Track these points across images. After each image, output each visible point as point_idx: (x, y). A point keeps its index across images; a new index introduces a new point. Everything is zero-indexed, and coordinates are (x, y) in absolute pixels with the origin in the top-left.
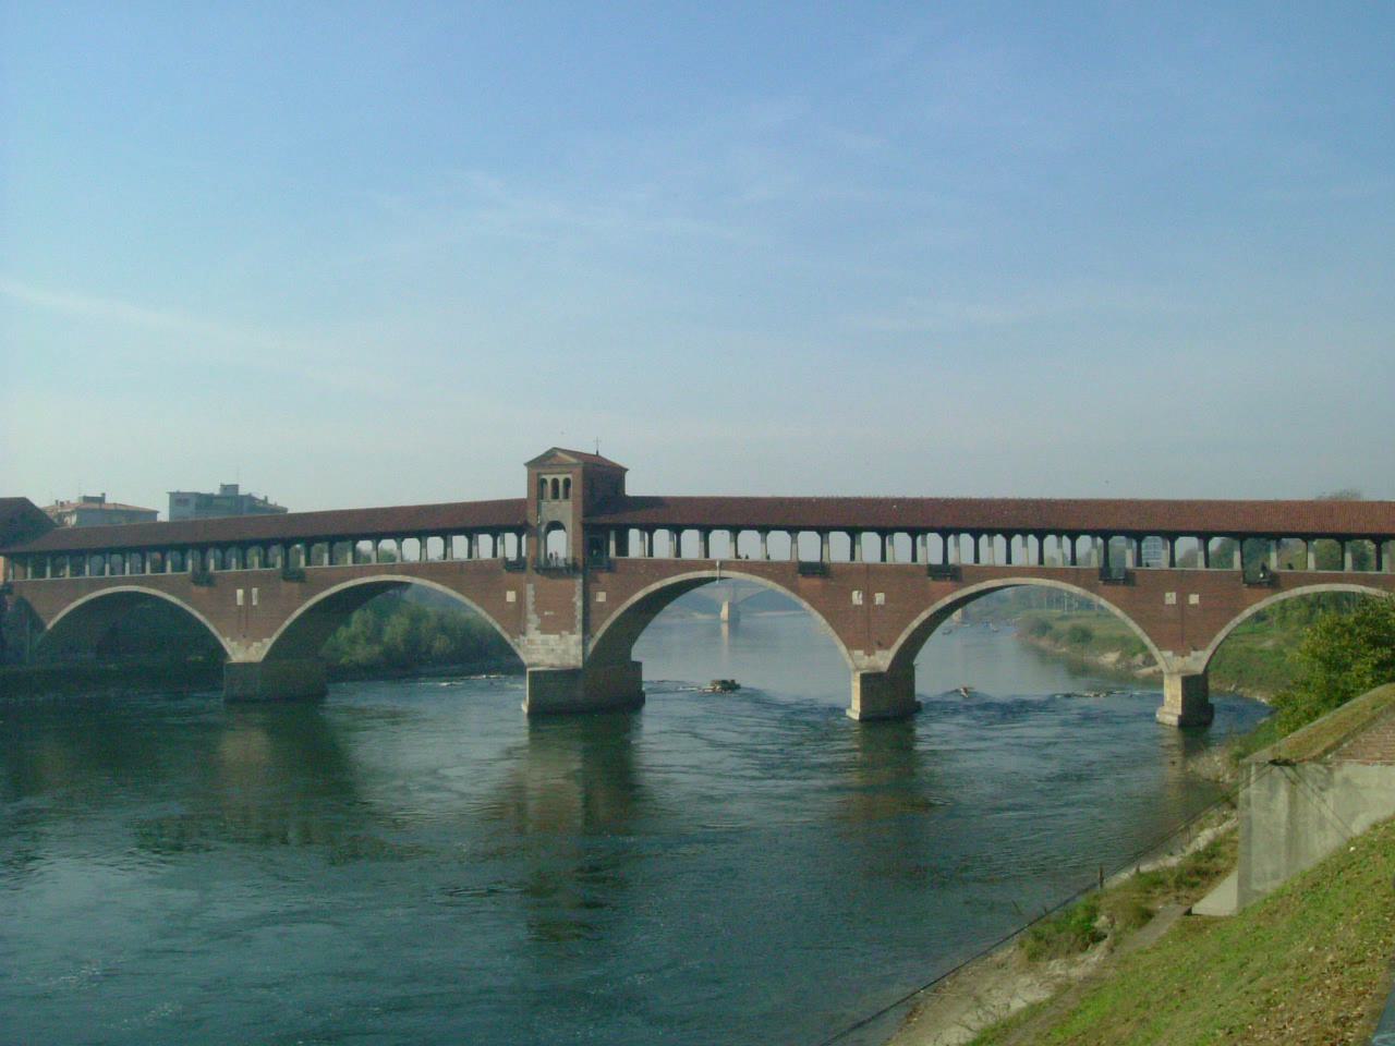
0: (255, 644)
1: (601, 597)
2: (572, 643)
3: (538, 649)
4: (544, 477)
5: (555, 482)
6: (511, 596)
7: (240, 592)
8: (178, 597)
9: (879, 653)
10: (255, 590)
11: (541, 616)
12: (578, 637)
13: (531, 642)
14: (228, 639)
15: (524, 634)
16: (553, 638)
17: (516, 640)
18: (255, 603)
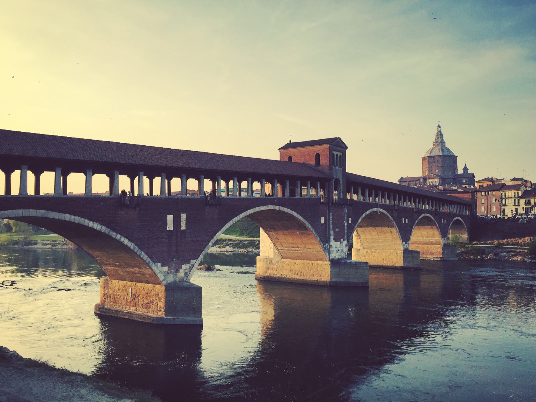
0: (184, 267)
1: (350, 222)
2: (344, 246)
3: (334, 251)
4: (333, 152)
5: (337, 155)
6: (323, 220)
7: (170, 218)
8: (101, 223)
9: (407, 242)
10: (183, 216)
11: (334, 231)
12: (345, 243)
13: (330, 246)
14: (159, 264)
15: (328, 241)
16: (339, 243)
17: (325, 246)
18: (183, 227)
